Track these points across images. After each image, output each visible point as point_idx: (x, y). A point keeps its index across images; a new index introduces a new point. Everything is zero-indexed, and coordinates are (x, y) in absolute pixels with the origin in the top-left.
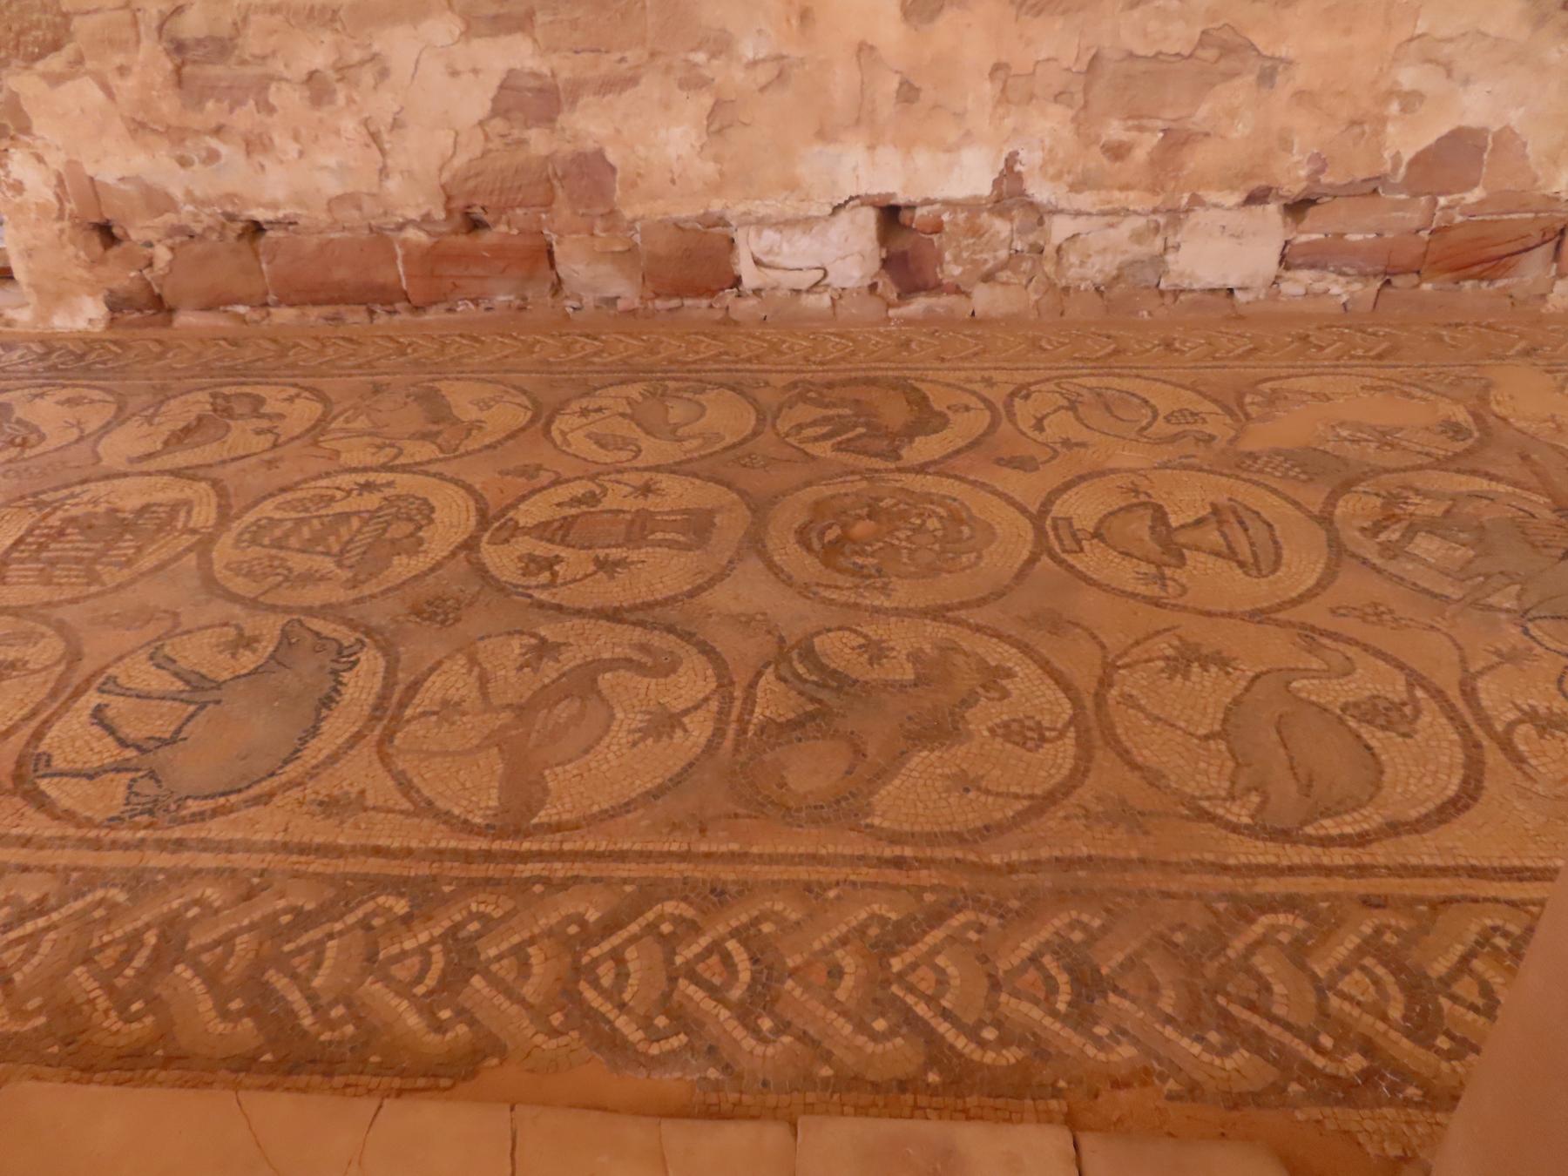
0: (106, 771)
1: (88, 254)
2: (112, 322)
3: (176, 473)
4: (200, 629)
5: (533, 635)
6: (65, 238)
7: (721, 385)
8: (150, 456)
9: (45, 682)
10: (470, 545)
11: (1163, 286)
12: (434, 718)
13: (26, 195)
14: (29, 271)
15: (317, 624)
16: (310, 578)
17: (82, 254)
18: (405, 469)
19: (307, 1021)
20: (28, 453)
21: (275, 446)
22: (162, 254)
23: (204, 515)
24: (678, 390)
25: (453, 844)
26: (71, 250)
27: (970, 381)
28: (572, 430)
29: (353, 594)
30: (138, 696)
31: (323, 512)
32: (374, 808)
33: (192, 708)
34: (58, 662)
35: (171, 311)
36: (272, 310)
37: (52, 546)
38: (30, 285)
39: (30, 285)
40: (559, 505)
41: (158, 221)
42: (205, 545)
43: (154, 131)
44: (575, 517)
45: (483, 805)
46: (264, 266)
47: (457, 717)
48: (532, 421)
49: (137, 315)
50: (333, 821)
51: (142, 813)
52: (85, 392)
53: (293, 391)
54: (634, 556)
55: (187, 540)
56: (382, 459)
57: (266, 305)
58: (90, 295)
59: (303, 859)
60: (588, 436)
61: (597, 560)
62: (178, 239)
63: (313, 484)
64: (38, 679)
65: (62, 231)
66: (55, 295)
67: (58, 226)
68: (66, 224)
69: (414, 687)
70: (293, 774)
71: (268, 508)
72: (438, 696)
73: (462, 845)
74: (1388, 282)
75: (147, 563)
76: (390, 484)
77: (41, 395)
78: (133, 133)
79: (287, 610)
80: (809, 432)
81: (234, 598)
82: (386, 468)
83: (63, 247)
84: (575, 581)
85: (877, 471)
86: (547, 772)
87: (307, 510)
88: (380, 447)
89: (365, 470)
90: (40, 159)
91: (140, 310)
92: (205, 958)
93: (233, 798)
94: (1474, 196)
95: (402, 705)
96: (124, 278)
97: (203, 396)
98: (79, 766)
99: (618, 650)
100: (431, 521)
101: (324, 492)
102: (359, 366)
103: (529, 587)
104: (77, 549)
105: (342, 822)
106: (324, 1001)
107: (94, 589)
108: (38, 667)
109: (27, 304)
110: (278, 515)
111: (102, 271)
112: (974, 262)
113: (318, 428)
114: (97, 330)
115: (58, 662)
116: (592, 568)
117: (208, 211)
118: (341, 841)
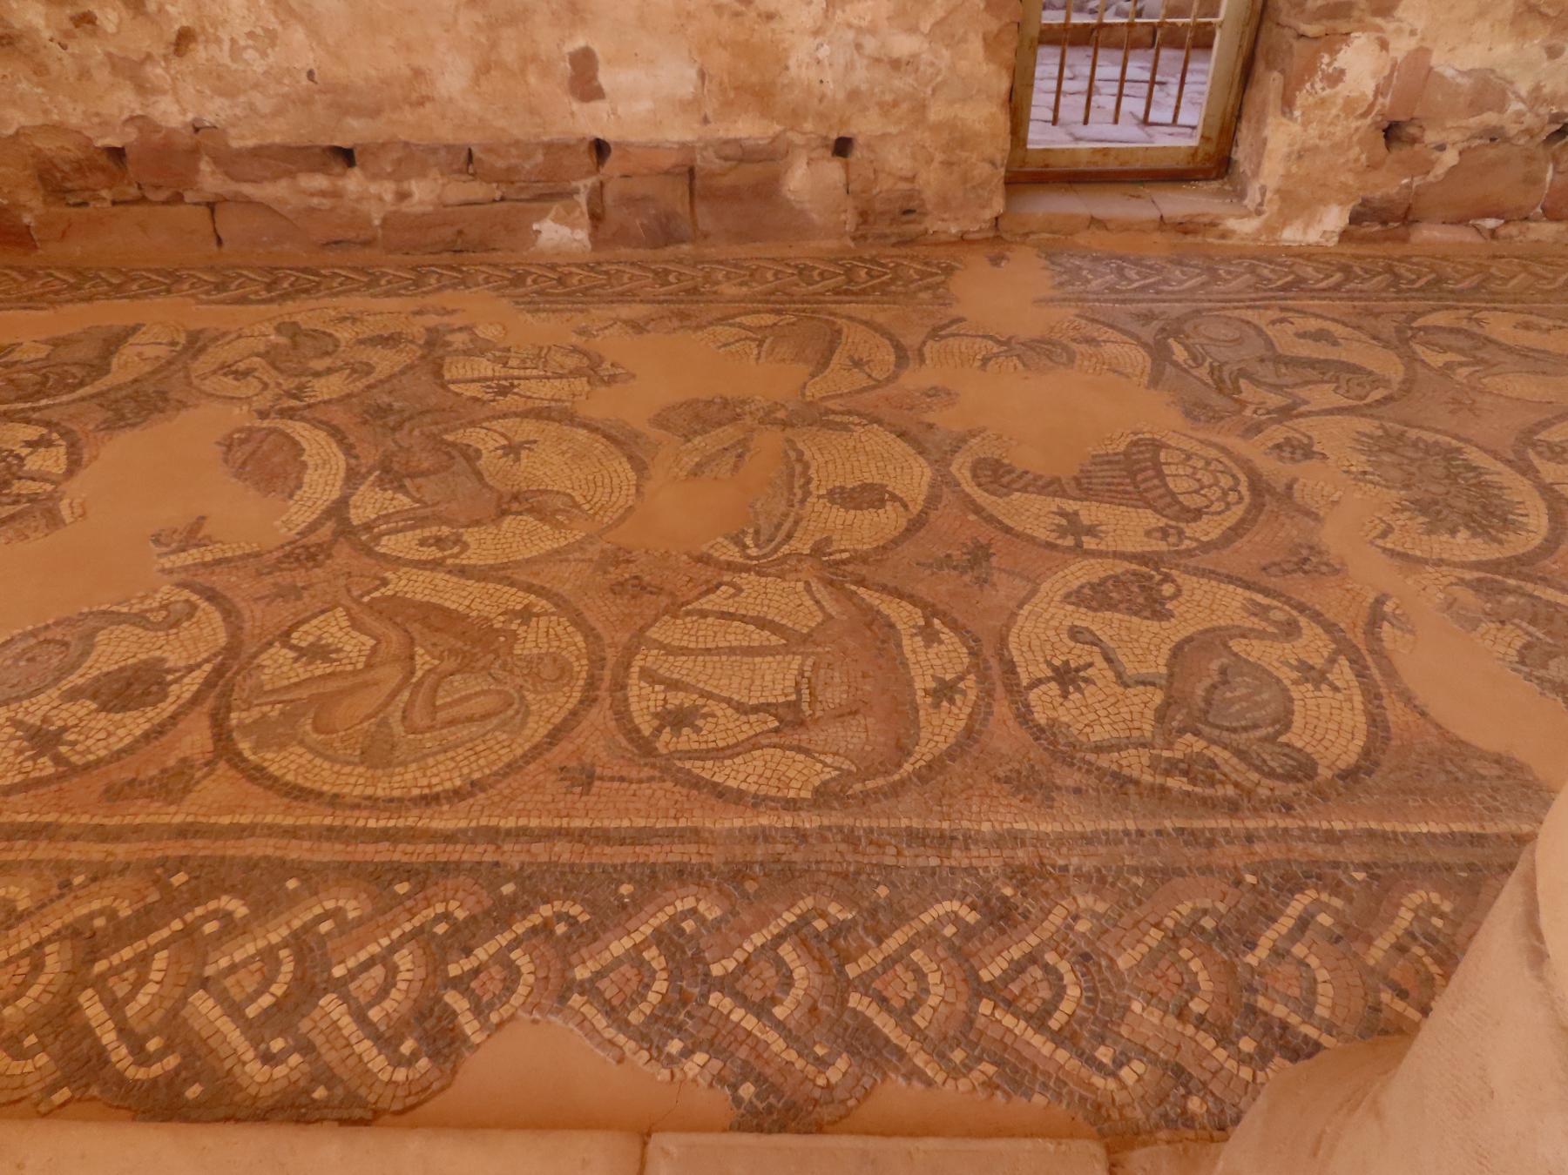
1: (1368, 158)
2: (1345, 236)
6: (1355, 138)
13: (1340, 87)
14: (1287, 176)
17: (1363, 157)
22: (1450, 158)
36: (1533, 225)
39: (1278, 191)
41: (1473, 121)
43: (1543, 15)
46: (1549, 175)
49: (1377, 228)
57: (1526, 219)
58: (1341, 204)
62: (1477, 142)
65: (1357, 129)
66: (1295, 202)
67: (1354, 124)
68: (1369, 120)
78: (1516, 20)
83: (1350, 148)
90: (1384, 45)
91: (1384, 223)
96: (1390, 185)
109: (1259, 213)
114: (1331, 244)
117: (1543, 111)
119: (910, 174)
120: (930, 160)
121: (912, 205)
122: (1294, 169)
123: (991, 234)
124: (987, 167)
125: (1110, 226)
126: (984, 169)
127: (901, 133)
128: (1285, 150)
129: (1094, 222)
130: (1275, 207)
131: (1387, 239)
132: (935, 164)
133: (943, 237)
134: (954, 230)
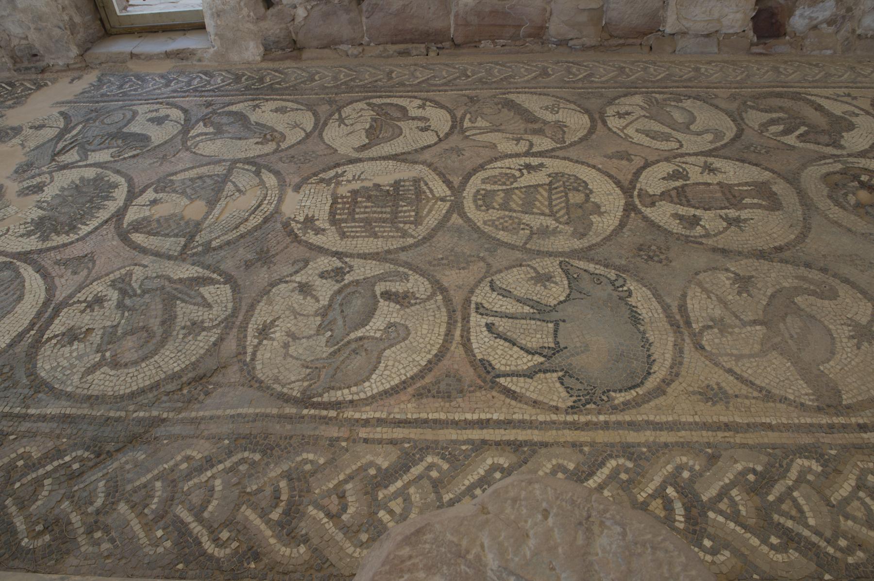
0: (536, 373)
1: (255, 14)
2: (265, 58)
3: (394, 157)
4: (507, 269)
5: (727, 270)
7: (690, 97)
8: (364, 148)
9: (438, 307)
10: (629, 208)
12: (716, 330)
14: (217, 26)
15: (582, 264)
16: (544, 232)
17: (252, 14)
18: (540, 154)
19: (830, 550)
20: (283, 146)
21: (440, 140)
23: (440, 188)
24: (665, 100)
25: (809, 420)
26: (245, 11)
27: (838, 96)
28: (625, 127)
29: (585, 243)
30: (506, 317)
31: (515, 185)
32: (736, 396)
33: (551, 325)
34: (433, 294)
35: (300, 49)
37: (357, 210)
38: (216, 35)
40: (664, 179)
42: (457, 207)
44: (683, 187)
45: (803, 392)
46: (364, 19)
47: (730, 330)
48: (592, 120)
50: (720, 407)
51: (589, 403)
52: (284, 104)
53: (419, 102)
54: (744, 214)
55: (444, 207)
56: (523, 147)
59: (726, 434)
60: (637, 131)
61: (726, 219)
63: (492, 165)
64: (431, 305)
69: (683, 308)
70: (664, 373)
71: (475, 183)
72: (705, 315)
73: (815, 421)
75: (431, 221)
76: (542, 165)
77: (258, 106)
79: (550, 254)
80: (773, 129)
81: (513, 247)
82: (527, 154)
83: (241, 9)
84: (721, 233)
86: (822, 368)
87: (504, 184)
88: (518, 140)
89: (517, 155)
91: (284, 50)
92: (723, 506)
93: (640, 391)
95: (688, 323)
97: (361, 105)
98: (513, 368)
99: (790, 281)
100: (591, 192)
101: (504, 171)
102: (445, 84)
103: (695, 237)
104: (375, 212)
105: (727, 408)
106: (828, 534)
107: (411, 241)
108: (423, 297)
110: (489, 187)
111: (264, 25)
112: (811, 18)
113: (456, 126)
115: (433, 294)
116: (725, 224)
118: (738, 420)
119: (24, 36)
120: (29, 28)
121: (34, 52)
122: (219, 23)
123: (84, 65)
124: (58, 30)
125: (143, 57)
126: (57, 32)
127: (8, 15)
128: (209, 12)
129: (132, 55)
130: (219, 43)
131: (287, 58)
132: (32, 30)
133: (57, 68)
134: (61, 63)
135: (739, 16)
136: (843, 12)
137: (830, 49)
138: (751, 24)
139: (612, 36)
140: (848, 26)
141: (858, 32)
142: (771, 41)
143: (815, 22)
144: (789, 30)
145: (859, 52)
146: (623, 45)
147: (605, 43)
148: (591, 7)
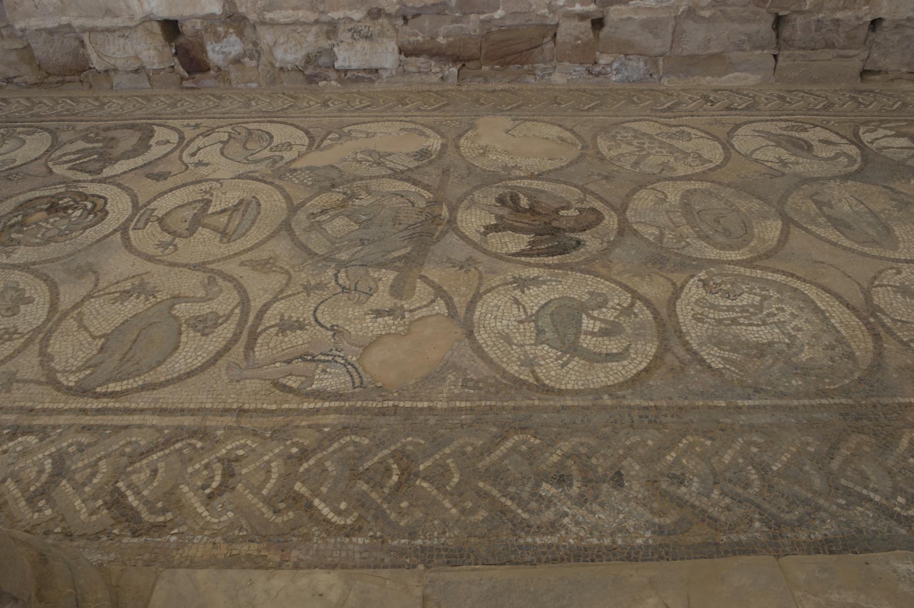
11: (336, 67)
74: (464, 65)
85: (79, 181)
94: (498, 14)
112: (223, 53)
135: (152, 53)
136: (250, 46)
137: (253, 82)
138: (176, 60)
139: (49, 74)
140: (263, 59)
141: (277, 65)
142: (198, 76)
143: (231, 57)
144: (211, 65)
145: (285, 84)
146: (63, 82)
147: (46, 80)
148: (14, 47)
